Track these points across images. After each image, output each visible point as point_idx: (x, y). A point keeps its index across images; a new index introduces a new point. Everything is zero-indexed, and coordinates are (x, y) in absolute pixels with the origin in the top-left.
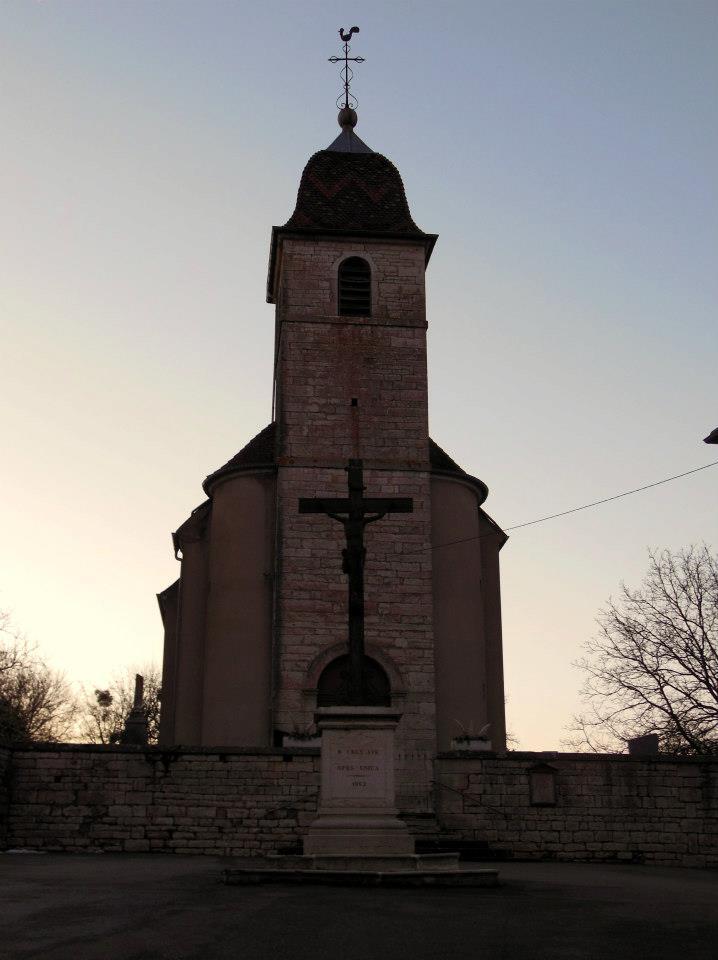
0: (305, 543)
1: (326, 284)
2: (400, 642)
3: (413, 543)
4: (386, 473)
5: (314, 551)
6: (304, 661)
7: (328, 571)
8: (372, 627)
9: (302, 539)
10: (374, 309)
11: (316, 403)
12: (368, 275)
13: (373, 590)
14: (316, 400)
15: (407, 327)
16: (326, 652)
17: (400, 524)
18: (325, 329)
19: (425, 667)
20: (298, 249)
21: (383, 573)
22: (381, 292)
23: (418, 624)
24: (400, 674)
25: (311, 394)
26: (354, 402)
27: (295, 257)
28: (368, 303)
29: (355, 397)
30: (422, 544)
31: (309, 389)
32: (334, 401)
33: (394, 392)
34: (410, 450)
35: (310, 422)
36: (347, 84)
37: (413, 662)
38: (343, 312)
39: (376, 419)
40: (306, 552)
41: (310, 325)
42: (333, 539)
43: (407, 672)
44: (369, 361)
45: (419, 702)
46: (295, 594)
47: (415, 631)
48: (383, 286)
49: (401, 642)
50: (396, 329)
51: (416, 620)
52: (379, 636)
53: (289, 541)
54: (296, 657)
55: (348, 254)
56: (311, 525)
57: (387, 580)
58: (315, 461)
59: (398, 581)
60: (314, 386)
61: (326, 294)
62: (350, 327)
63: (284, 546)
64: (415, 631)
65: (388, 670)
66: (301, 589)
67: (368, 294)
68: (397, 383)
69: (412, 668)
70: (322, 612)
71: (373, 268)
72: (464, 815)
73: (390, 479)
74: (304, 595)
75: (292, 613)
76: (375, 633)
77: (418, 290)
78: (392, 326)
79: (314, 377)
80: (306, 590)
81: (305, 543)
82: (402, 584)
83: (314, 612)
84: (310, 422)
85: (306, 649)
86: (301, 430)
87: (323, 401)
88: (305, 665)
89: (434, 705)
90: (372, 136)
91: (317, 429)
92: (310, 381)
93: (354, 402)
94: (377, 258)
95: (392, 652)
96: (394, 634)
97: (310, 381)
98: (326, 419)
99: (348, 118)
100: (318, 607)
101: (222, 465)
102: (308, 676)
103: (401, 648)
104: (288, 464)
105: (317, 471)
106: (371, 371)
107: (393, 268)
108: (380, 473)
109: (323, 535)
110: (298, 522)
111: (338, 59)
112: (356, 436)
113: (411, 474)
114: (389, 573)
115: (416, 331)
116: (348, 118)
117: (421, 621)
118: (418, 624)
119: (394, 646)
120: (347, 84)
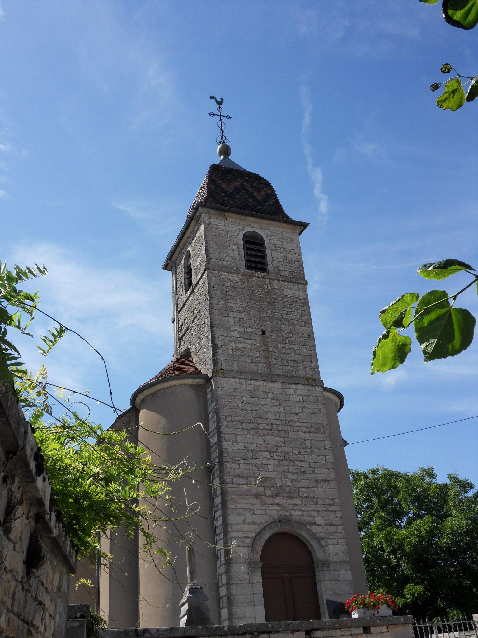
0: (239, 438)
1: (235, 247)
2: (319, 520)
3: (318, 441)
4: (293, 386)
5: (246, 445)
6: (247, 537)
7: (259, 462)
8: (296, 508)
9: (236, 435)
10: (270, 268)
11: (236, 330)
12: (262, 244)
13: (294, 477)
14: (236, 328)
15: (293, 283)
16: (264, 529)
17: (306, 425)
18: (237, 278)
19: (339, 540)
20: (213, 220)
21: (299, 464)
22: (272, 257)
23: (330, 505)
24: (322, 546)
25: (232, 323)
26: (263, 333)
27: (211, 226)
28: (264, 263)
29: (264, 328)
30: (324, 441)
31: (231, 319)
32: (248, 330)
33: (291, 327)
34: (307, 370)
35: (233, 344)
36: (222, 130)
37: (331, 537)
38: (249, 267)
39: (280, 346)
40: (239, 446)
41: (226, 274)
42: (260, 435)
43: (327, 546)
44: (270, 303)
45: (339, 571)
46: (235, 480)
47: (328, 511)
48: (274, 253)
49: (319, 520)
50: (286, 283)
51: (328, 502)
52: (302, 515)
53: (226, 436)
54: (240, 534)
55: (247, 229)
56: (242, 424)
57: (303, 470)
58: (241, 374)
59: (311, 470)
60: (234, 318)
61: (236, 254)
62: (255, 278)
63: (223, 440)
64: (328, 511)
65: (314, 544)
66: (239, 476)
67: (264, 257)
68: (292, 321)
69: (330, 542)
70: (257, 496)
71: (266, 241)
72: (264, 508)
73: (295, 390)
74: (242, 481)
75: (234, 496)
76: (299, 513)
77: (298, 259)
78: (283, 281)
79: (234, 312)
80: (243, 477)
81: (239, 438)
82: (314, 472)
83: (251, 495)
84: (233, 344)
85: (247, 527)
86: (228, 350)
87: (241, 330)
88: (248, 541)
89: (349, 572)
90: (243, 159)
91: (238, 350)
92: (231, 314)
93: (263, 333)
94: (268, 231)
95: (314, 529)
96: (314, 514)
97: (231, 314)
98: (244, 342)
99: (226, 151)
100: (254, 491)
101: (161, 369)
102: (252, 550)
103: (319, 525)
104: (221, 375)
105: (242, 381)
106: (273, 311)
107: (279, 243)
108: (288, 386)
109: (252, 432)
110: (232, 421)
111: (214, 115)
112: (267, 356)
113: (309, 388)
114: (303, 464)
115: (300, 286)
116: (226, 151)
117: (331, 502)
118: (330, 505)
119: (314, 524)
120: (222, 130)
